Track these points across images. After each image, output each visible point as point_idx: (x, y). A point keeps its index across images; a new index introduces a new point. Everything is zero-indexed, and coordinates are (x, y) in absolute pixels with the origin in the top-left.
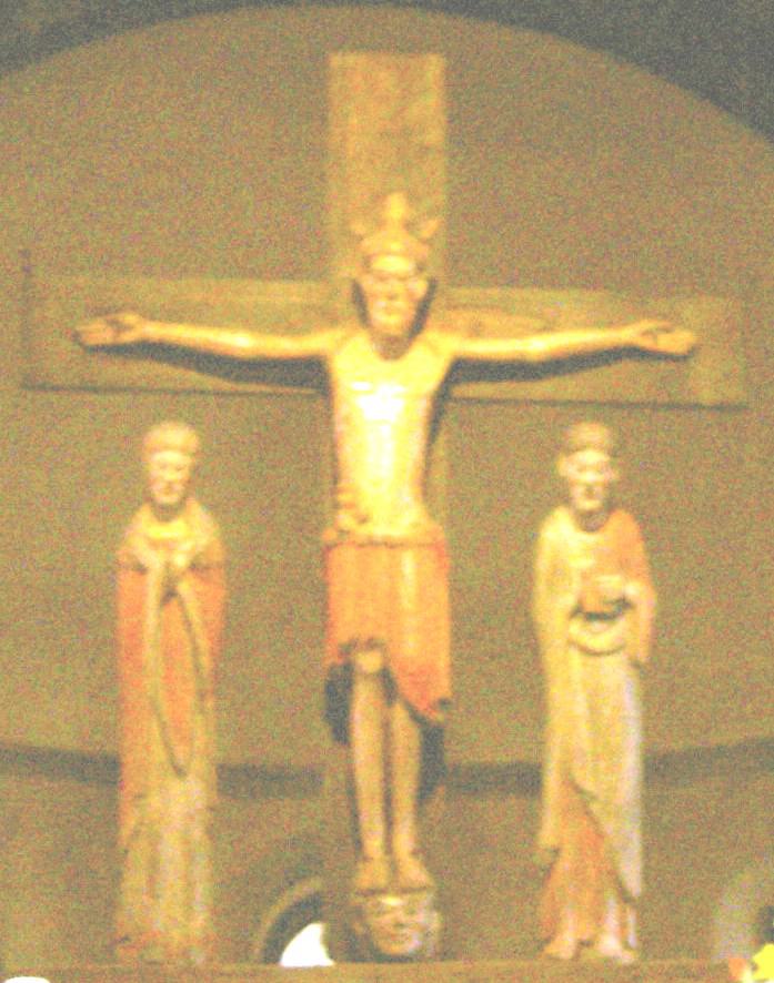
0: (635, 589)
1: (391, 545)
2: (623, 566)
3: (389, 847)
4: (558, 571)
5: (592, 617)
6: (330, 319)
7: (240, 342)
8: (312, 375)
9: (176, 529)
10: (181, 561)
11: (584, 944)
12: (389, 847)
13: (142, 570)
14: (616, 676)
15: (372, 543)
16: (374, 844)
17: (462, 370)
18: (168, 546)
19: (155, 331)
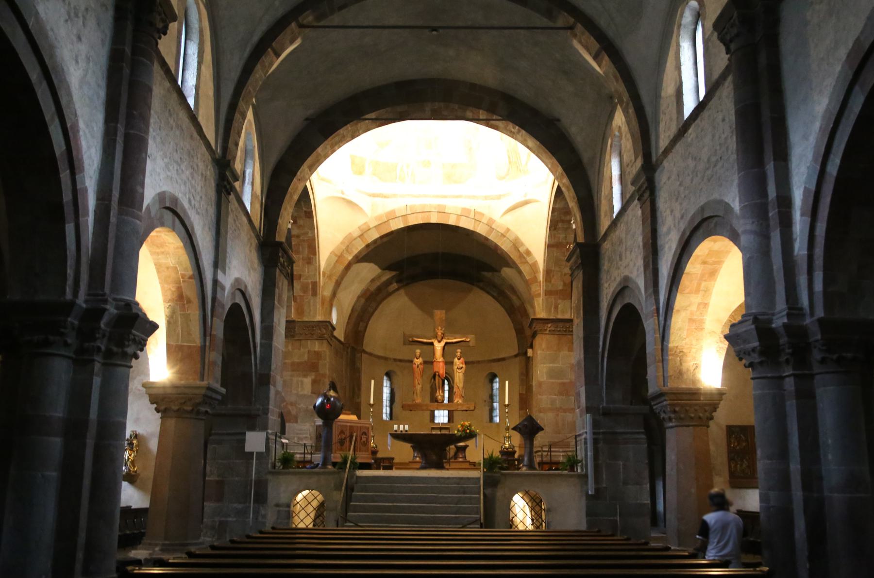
0: (464, 366)
1: (439, 362)
2: (462, 364)
3: (439, 392)
4: (456, 364)
5: (459, 369)
6: (434, 338)
7: (425, 340)
8: (432, 344)
9: (418, 360)
10: (419, 363)
11: (457, 401)
12: (439, 392)
13: (415, 364)
14: (461, 374)
15: (438, 362)
16: (438, 392)
17: (447, 343)
18: (417, 362)
19: (416, 339)
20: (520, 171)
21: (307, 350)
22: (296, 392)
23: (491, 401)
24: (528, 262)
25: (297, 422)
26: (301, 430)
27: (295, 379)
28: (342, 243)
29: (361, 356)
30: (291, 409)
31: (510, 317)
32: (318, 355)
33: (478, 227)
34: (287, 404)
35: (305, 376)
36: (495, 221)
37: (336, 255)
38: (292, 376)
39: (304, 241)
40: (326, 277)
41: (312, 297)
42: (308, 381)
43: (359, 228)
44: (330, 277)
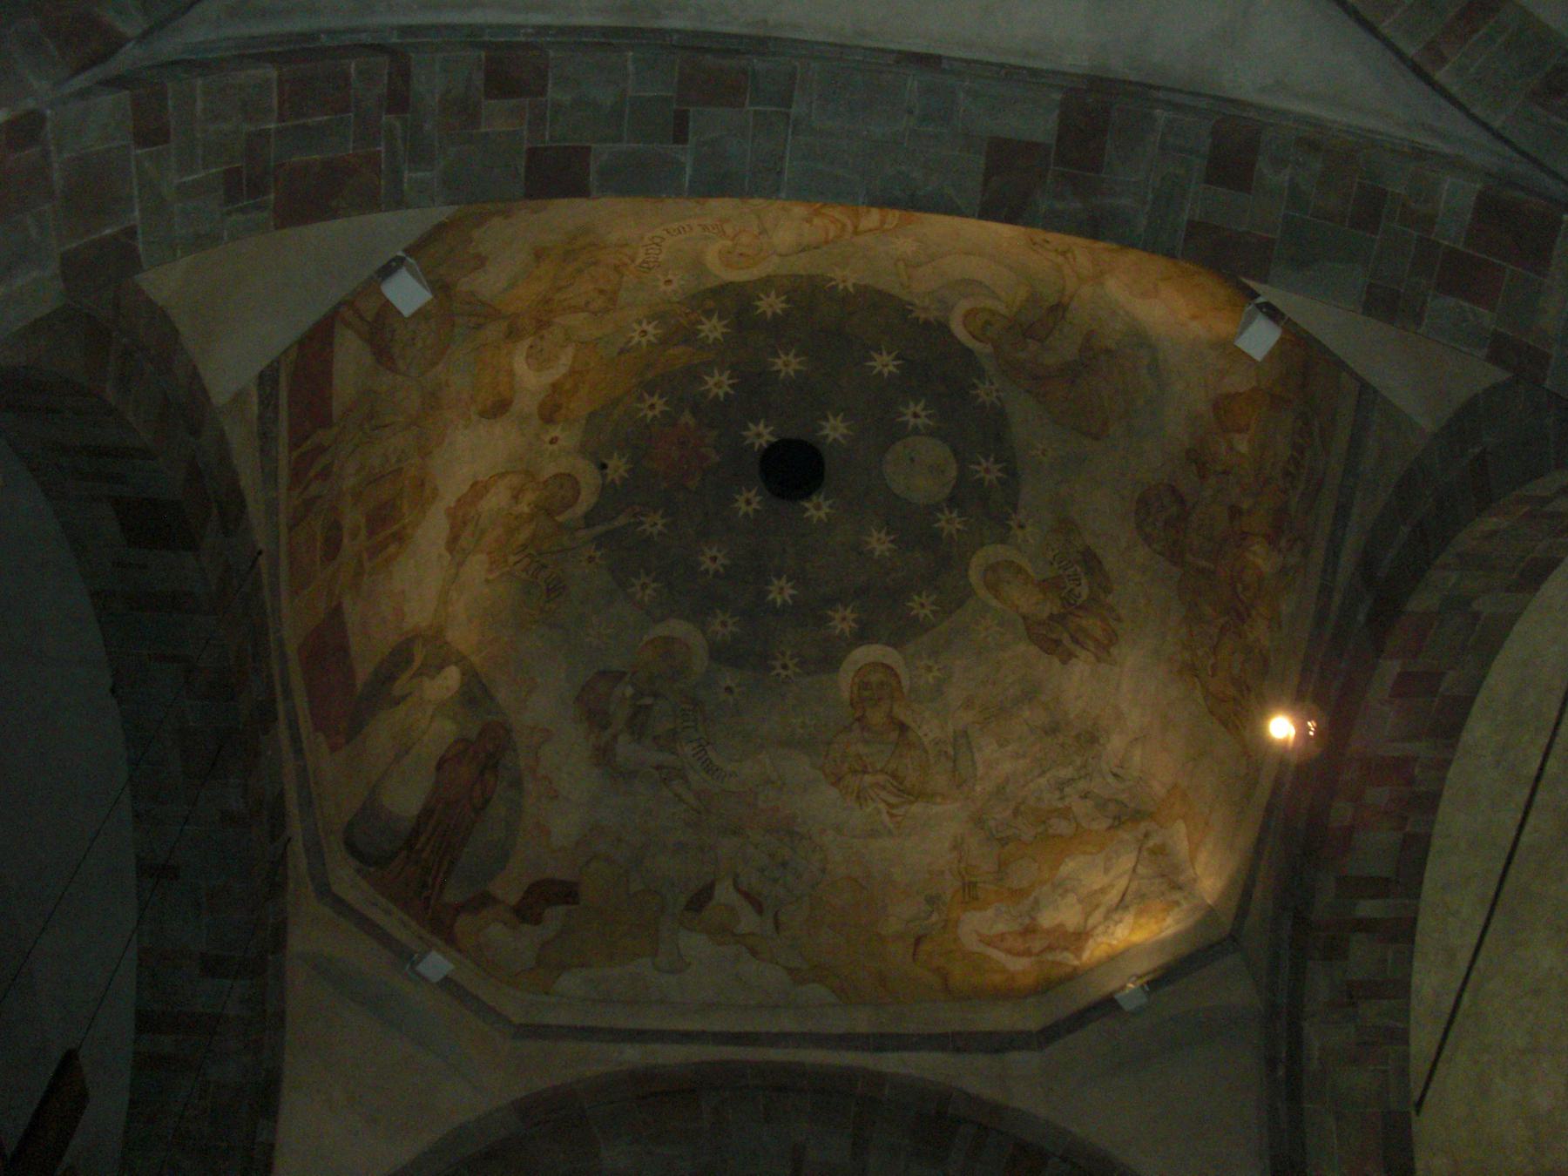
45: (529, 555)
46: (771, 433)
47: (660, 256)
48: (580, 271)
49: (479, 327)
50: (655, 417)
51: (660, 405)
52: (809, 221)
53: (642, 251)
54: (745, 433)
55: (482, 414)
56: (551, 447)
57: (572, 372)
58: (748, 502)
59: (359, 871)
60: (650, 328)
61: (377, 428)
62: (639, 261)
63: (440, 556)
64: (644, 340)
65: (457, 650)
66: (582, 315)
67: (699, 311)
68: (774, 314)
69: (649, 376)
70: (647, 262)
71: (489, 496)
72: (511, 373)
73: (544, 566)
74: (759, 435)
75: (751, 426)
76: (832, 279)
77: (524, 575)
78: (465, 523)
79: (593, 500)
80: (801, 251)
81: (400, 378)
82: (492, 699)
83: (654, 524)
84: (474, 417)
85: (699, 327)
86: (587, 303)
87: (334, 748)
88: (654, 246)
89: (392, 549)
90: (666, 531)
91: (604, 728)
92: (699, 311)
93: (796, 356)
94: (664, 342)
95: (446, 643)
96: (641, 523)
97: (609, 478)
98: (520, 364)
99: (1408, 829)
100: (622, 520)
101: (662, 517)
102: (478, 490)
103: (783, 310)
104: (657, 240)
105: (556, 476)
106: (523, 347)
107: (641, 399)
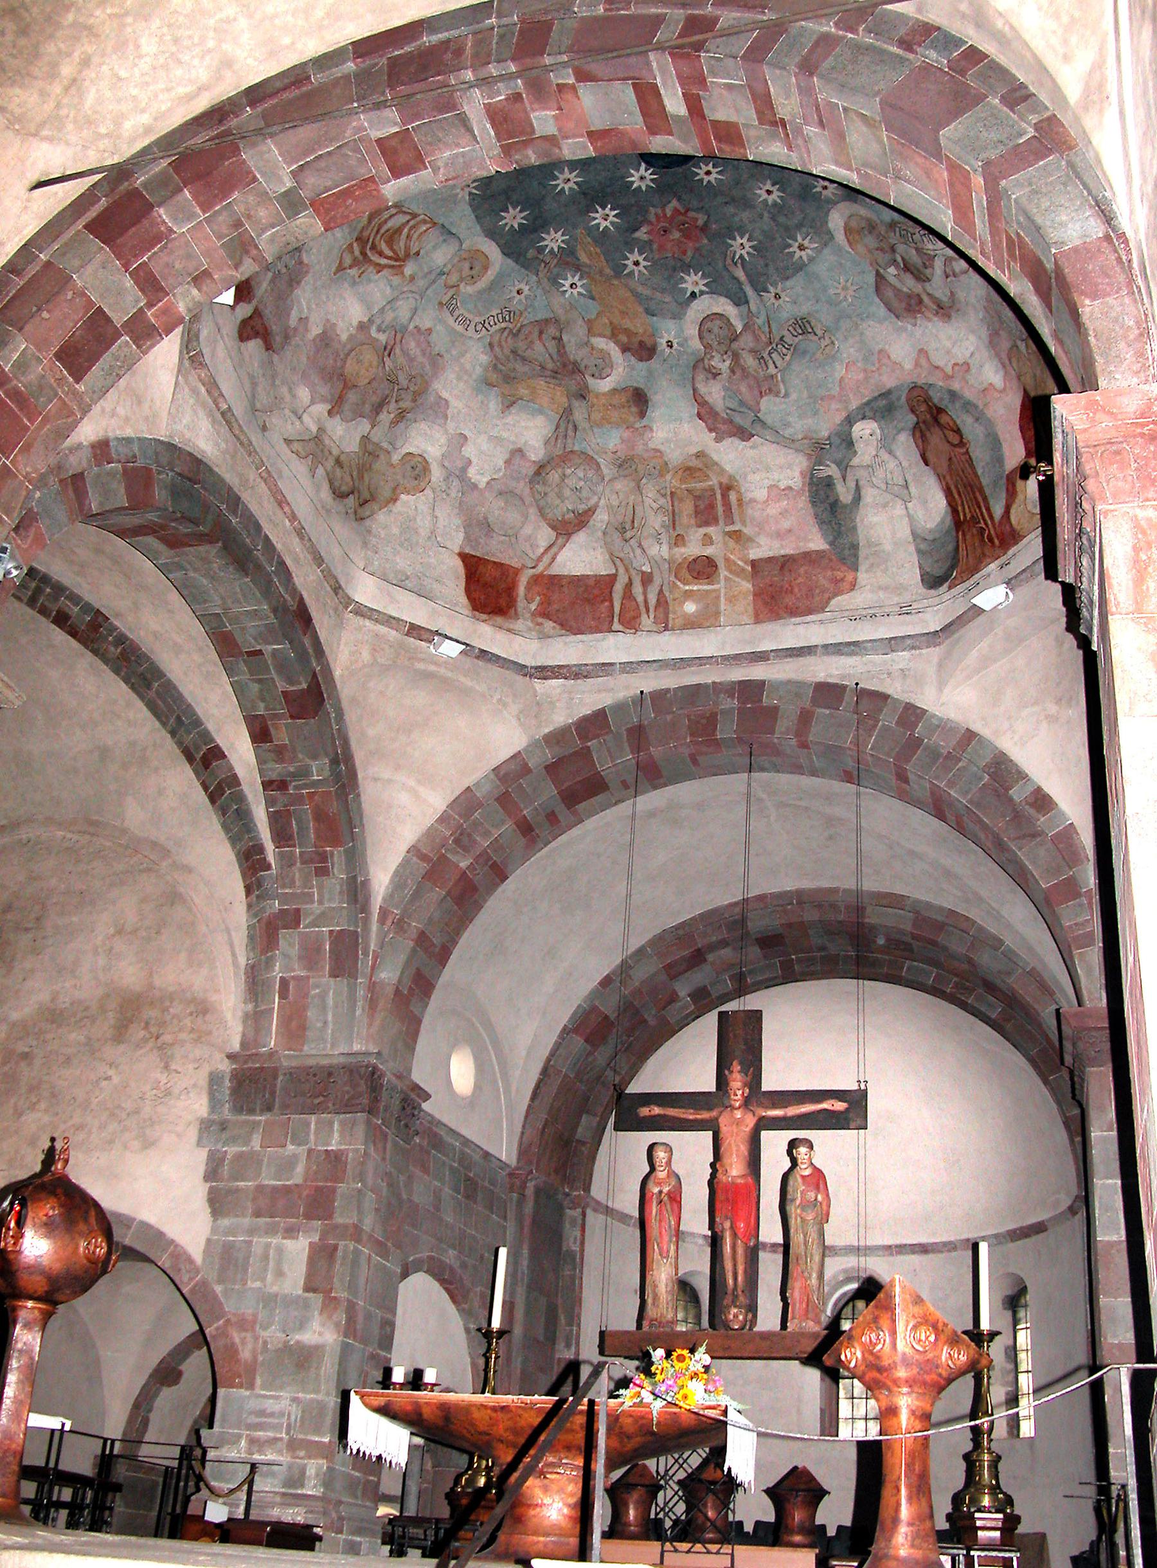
20: (991, 540)
21: (302, 1150)
22: (258, 1284)
23: (1011, 1366)
24: (1041, 834)
25: (251, 1386)
26: (262, 1413)
27: (259, 1241)
28: (443, 819)
29: (584, 1214)
30: (237, 1340)
31: (1046, 1082)
32: (335, 1160)
33: (871, 736)
34: (228, 1321)
35: (291, 1232)
36: (924, 711)
37: (424, 857)
38: (252, 1231)
39: (299, 799)
40: (389, 922)
41: (332, 980)
42: (298, 1248)
43: (495, 770)
44: (400, 925)
45: (770, 354)
46: (638, 170)
47: (494, 313)
48: (524, 359)
49: (575, 428)
50: (644, 259)
51: (635, 256)
52: (418, 254)
53: (492, 330)
54: (644, 188)
55: (642, 414)
56: (675, 345)
57: (613, 336)
58: (708, 173)
59: (950, 588)
60: (567, 284)
61: (633, 522)
62: (503, 325)
63: (751, 447)
64: (579, 284)
65: (841, 424)
66: (565, 338)
67: (541, 257)
68: (521, 211)
69: (608, 271)
70: (504, 319)
71: (710, 401)
72: (614, 391)
73: (782, 339)
74: (642, 178)
75: (635, 185)
76: (470, 194)
77: (787, 358)
78: (731, 422)
79: (723, 300)
80: (451, 233)
81: (602, 502)
82: (889, 392)
83: (742, 246)
84: (645, 422)
85: (556, 250)
86: (554, 338)
87: (853, 586)
88: (486, 325)
89: (733, 496)
90: (747, 236)
91: (921, 302)
92: (541, 257)
93: (556, 178)
94: (578, 268)
95: (829, 438)
96: (741, 257)
97: (704, 288)
98: (605, 385)
99: (571, 80)
100: (740, 274)
101: (734, 239)
102: (706, 413)
103: (514, 208)
104: (479, 327)
105: (701, 338)
106: (591, 381)
107: (632, 273)
